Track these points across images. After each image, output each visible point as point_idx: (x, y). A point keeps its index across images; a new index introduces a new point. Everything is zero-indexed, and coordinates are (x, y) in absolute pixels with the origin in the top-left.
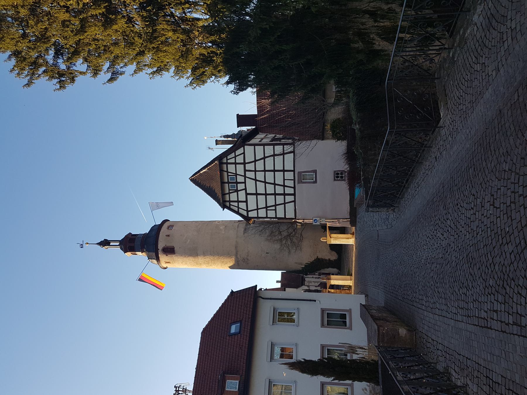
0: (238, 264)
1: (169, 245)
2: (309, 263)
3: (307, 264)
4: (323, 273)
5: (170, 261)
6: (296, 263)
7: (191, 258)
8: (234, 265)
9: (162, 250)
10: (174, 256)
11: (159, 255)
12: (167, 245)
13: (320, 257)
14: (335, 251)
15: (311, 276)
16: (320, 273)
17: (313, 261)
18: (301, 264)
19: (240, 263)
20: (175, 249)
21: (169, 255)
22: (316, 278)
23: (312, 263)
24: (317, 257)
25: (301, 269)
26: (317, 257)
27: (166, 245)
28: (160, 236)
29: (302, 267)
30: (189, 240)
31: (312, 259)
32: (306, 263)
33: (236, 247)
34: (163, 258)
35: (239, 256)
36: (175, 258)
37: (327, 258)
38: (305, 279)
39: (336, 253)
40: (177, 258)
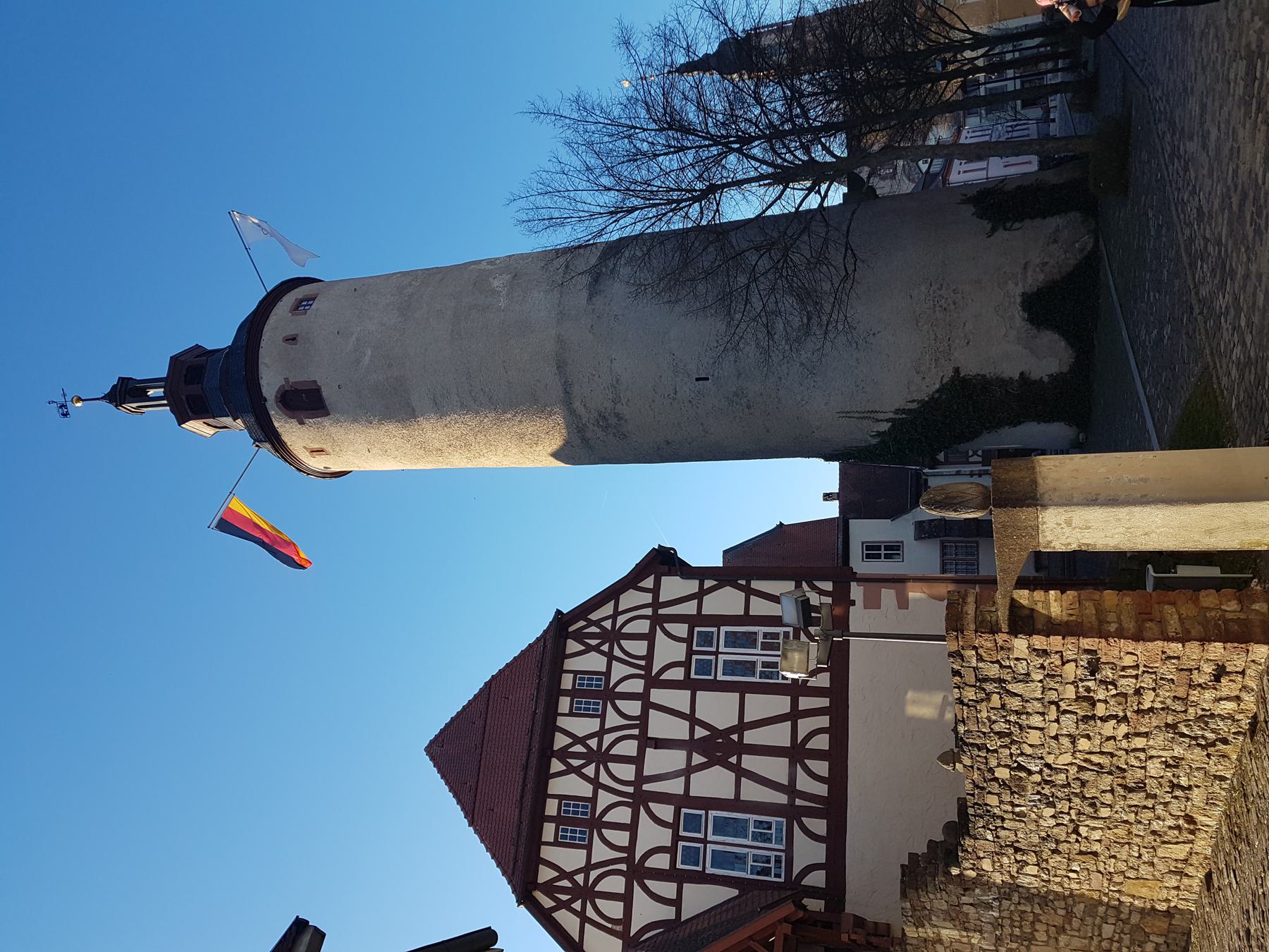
0: (585, 440)
1: (299, 377)
2: (914, 406)
3: (904, 411)
4: (999, 451)
5: (324, 447)
6: (847, 414)
7: (392, 428)
8: (567, 443)
9: (276, 402)
10: (326, 421)
11: (276, 424)
12: (291, 380)
13: (971, 367)
14: (1056, 328)
15: (953, 469)
16: (990, 451)
17: (932, 398)
18: (871, 415)
19: (589, 435)
20: (325, 394)
21: (307, 421)
22: (972, 474)
23: (929, 407)
24: (957, 370)
25: (874, 441)
26: (957, 370)
27: (286, 380)
28: (263, 344)
29: (879, 434)
30: (369, 352)
31: (928, 386)
32: (897, 411)
33: (561, 366)
34: (295, 435)
35: (577, 404)
36: (333, 430)
37: (1011, 371)
38: (926, 481)
39: (1065, 334)
40: (342, 431)
